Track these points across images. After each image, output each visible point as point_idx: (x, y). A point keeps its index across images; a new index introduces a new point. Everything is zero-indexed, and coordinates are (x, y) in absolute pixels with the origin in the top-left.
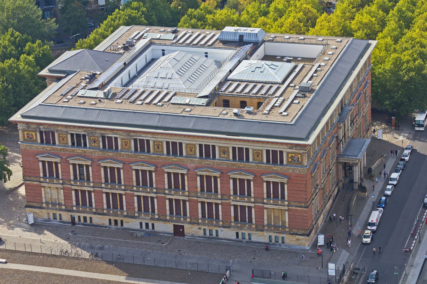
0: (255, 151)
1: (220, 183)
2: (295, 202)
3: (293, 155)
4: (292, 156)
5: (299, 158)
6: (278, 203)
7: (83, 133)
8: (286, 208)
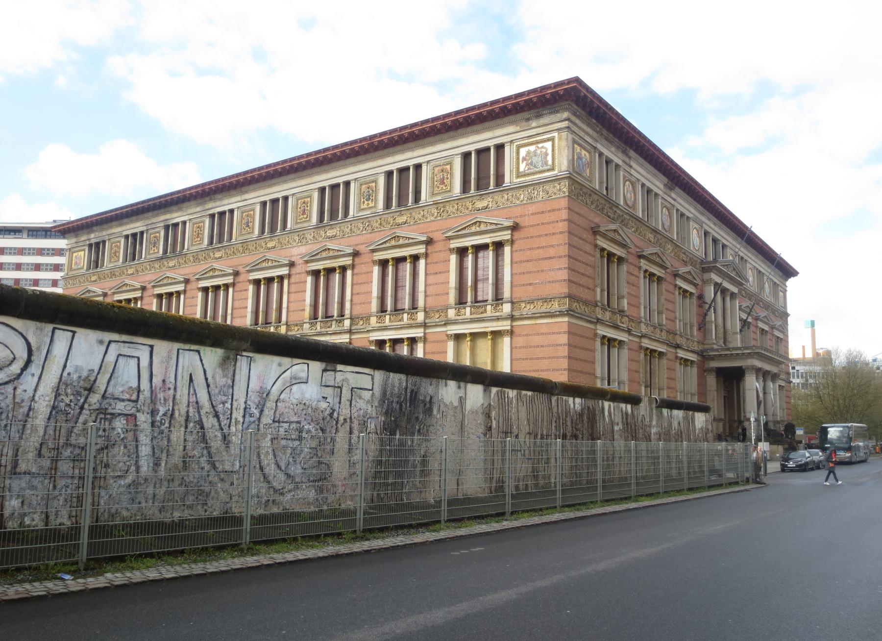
0: (436, 169)
1: (353, 285)
2: (531, 302)
3: (532, 148)
4: (528, 152)
5: (547, 154)
6: (485, 311)
7: (141, 229)
8: (505, 325)
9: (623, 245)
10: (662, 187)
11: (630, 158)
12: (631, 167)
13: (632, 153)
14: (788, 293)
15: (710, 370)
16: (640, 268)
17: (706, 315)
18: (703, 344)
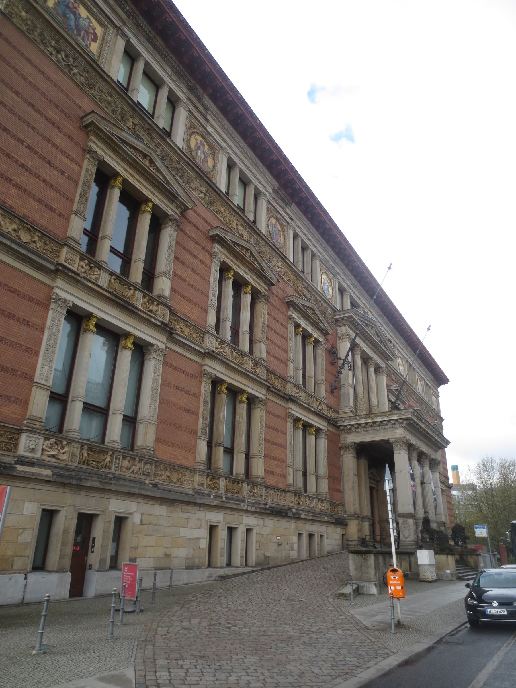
9: (171, 196)
10: (271, 191)
11: (206, 109)
12: (207, 120)
13: (207, 100)
14: (440, 399)
15: (347, 447)
16: (212, 255)
17: (339, 373)
18: (338, 412)
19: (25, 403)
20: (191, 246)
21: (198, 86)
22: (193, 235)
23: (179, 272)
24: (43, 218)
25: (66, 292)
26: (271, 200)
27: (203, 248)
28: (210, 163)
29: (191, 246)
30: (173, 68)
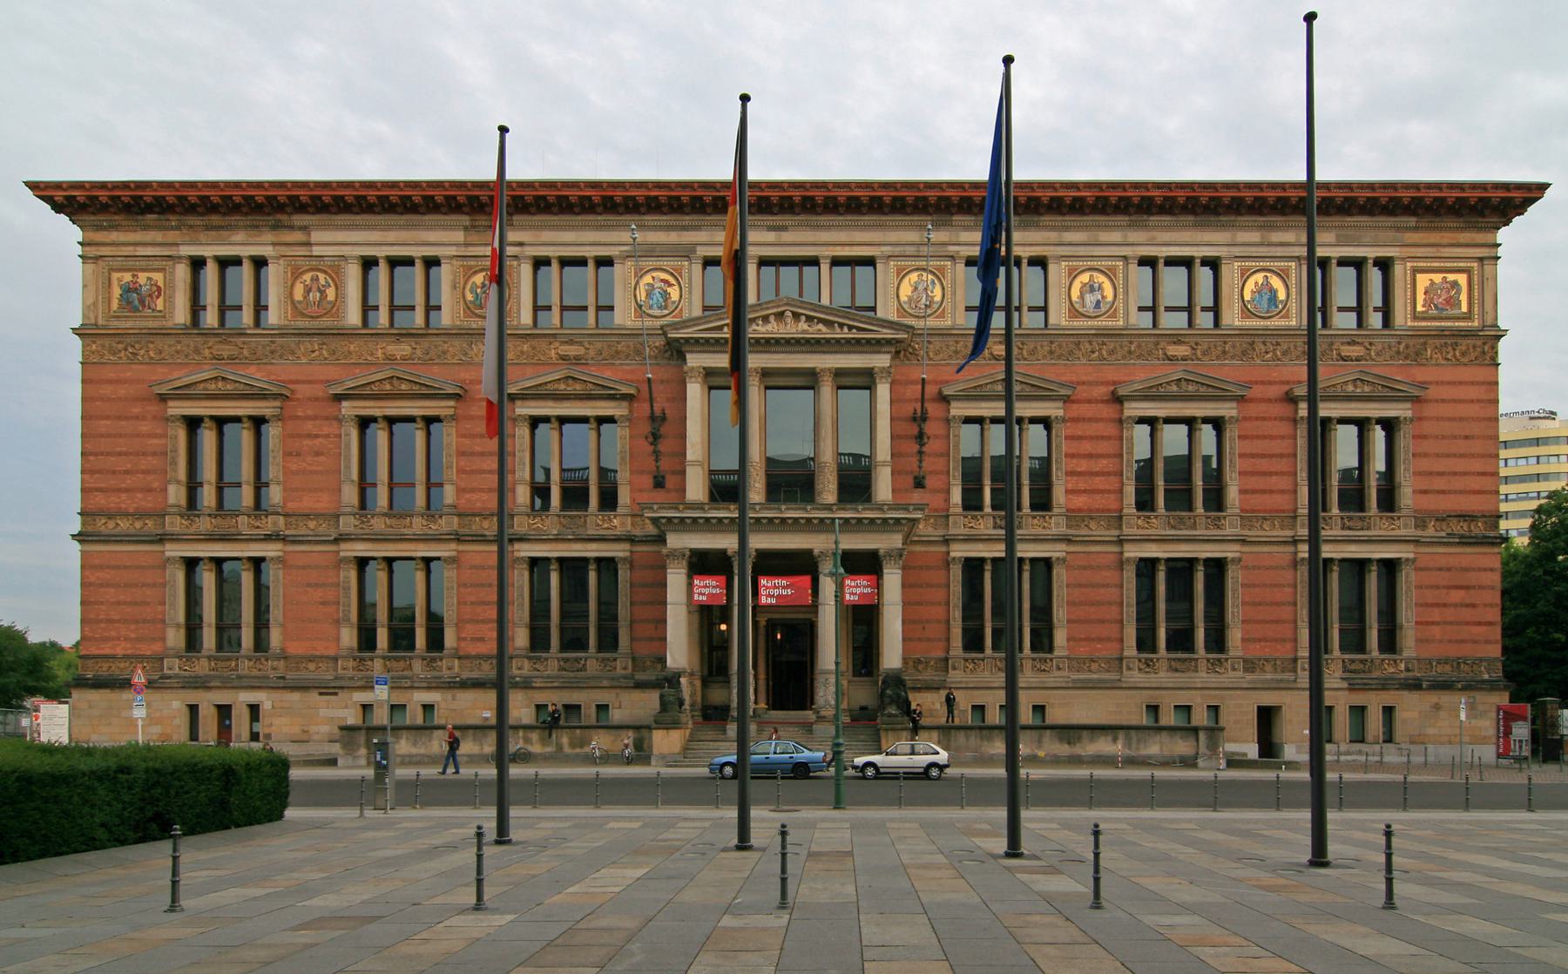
9: (262, 396)
10: (459, 236)
11: (305, 229)
13: (299, 219)
19: (163, 639)
20: (309, 426)
21: (279, 216)
22: (310, 412)
23: (294, 467)
24: (148, 503)
25: (175, 551)
26: (462, 251)
27: (327, 418)
28: (331, 294)
29: (309, 426)
30: (246, 227)
